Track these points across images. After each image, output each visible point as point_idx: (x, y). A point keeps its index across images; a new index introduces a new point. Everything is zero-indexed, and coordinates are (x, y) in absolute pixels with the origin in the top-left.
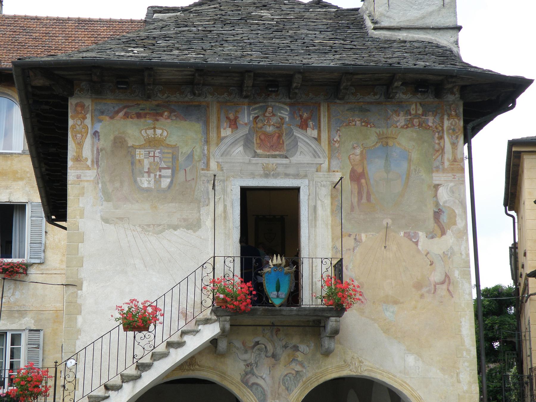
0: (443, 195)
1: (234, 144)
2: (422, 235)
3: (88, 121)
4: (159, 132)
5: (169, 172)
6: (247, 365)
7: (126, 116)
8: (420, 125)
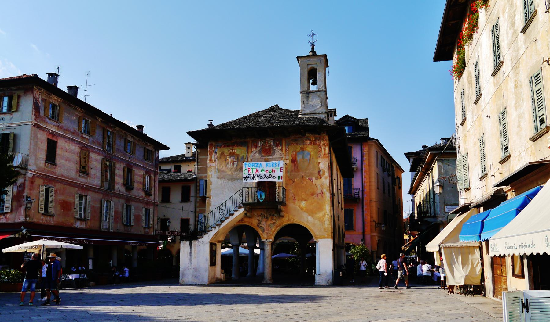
0: (321, 166)
2: (314, 179)
3: (214, 149)
6: (259, 221)
7: (224, 147)
8: (314, 144)
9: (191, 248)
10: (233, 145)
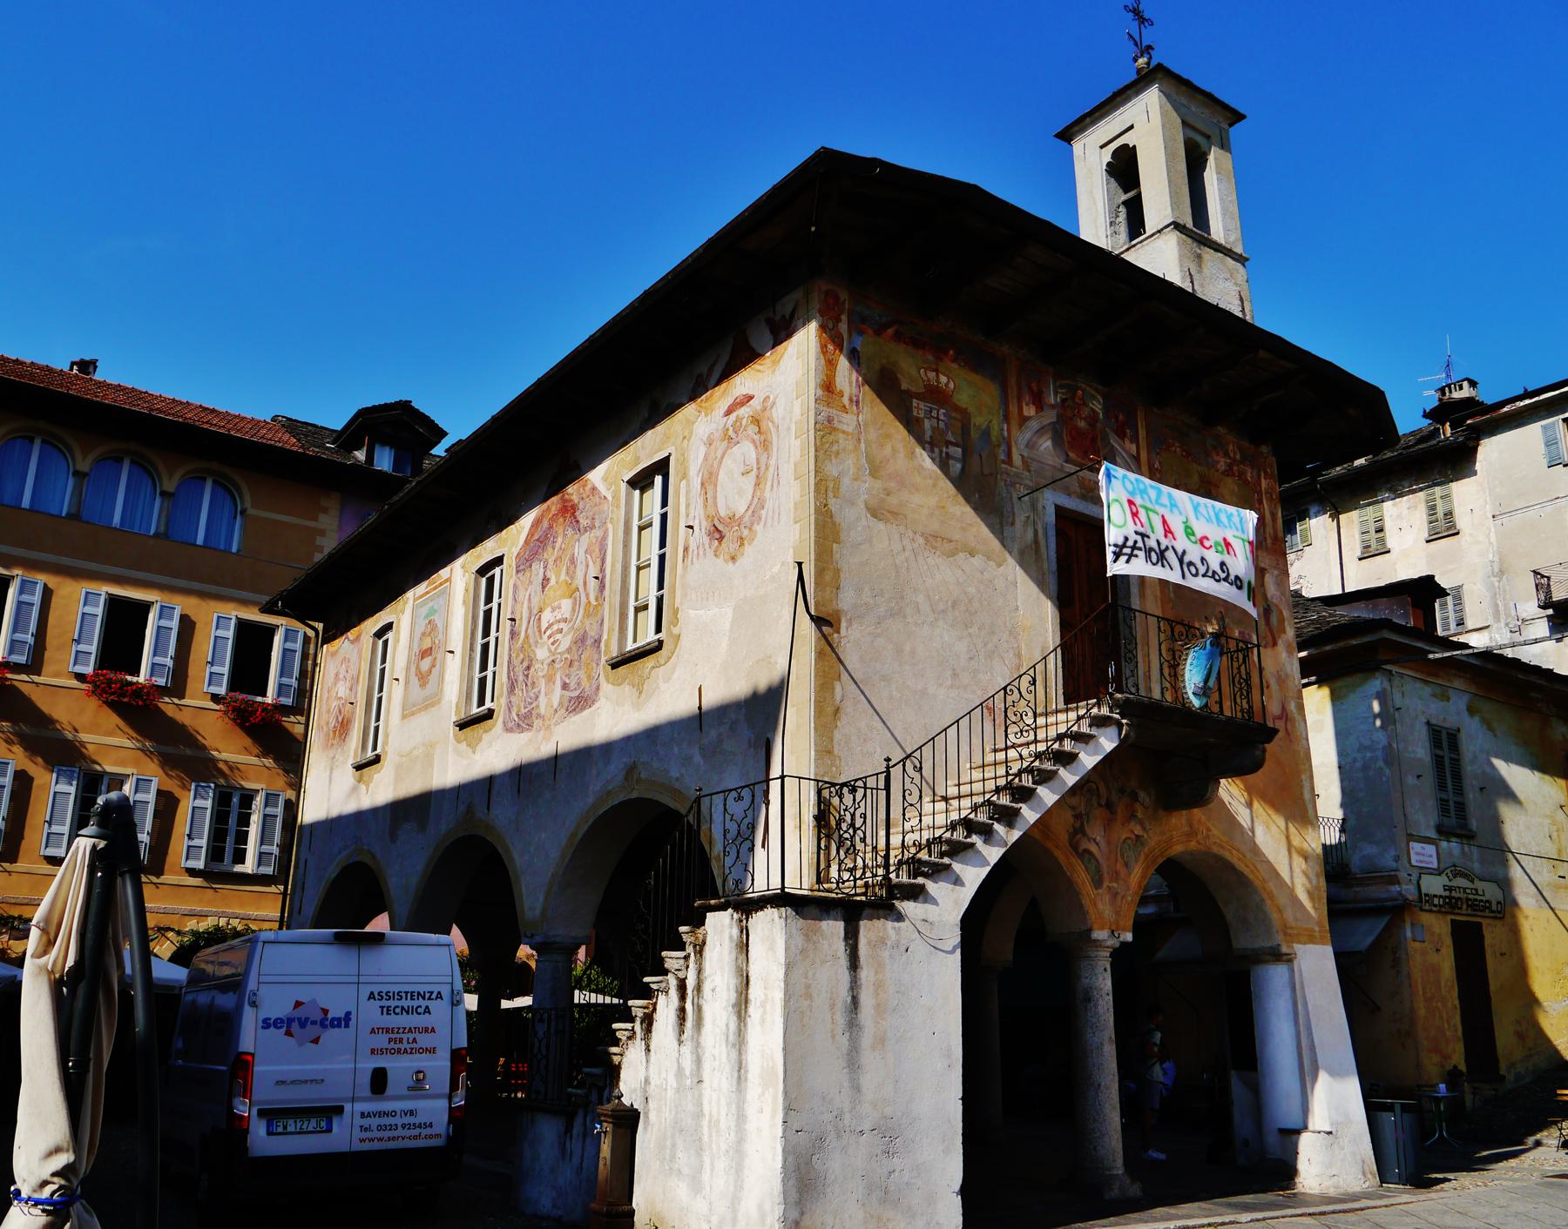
1: (1040, 431)
4: (943, 379)
5: (957, 451)
6: (1077, 817)
7: (898, 337)
9: (854, 963)
10: (938, 348)
